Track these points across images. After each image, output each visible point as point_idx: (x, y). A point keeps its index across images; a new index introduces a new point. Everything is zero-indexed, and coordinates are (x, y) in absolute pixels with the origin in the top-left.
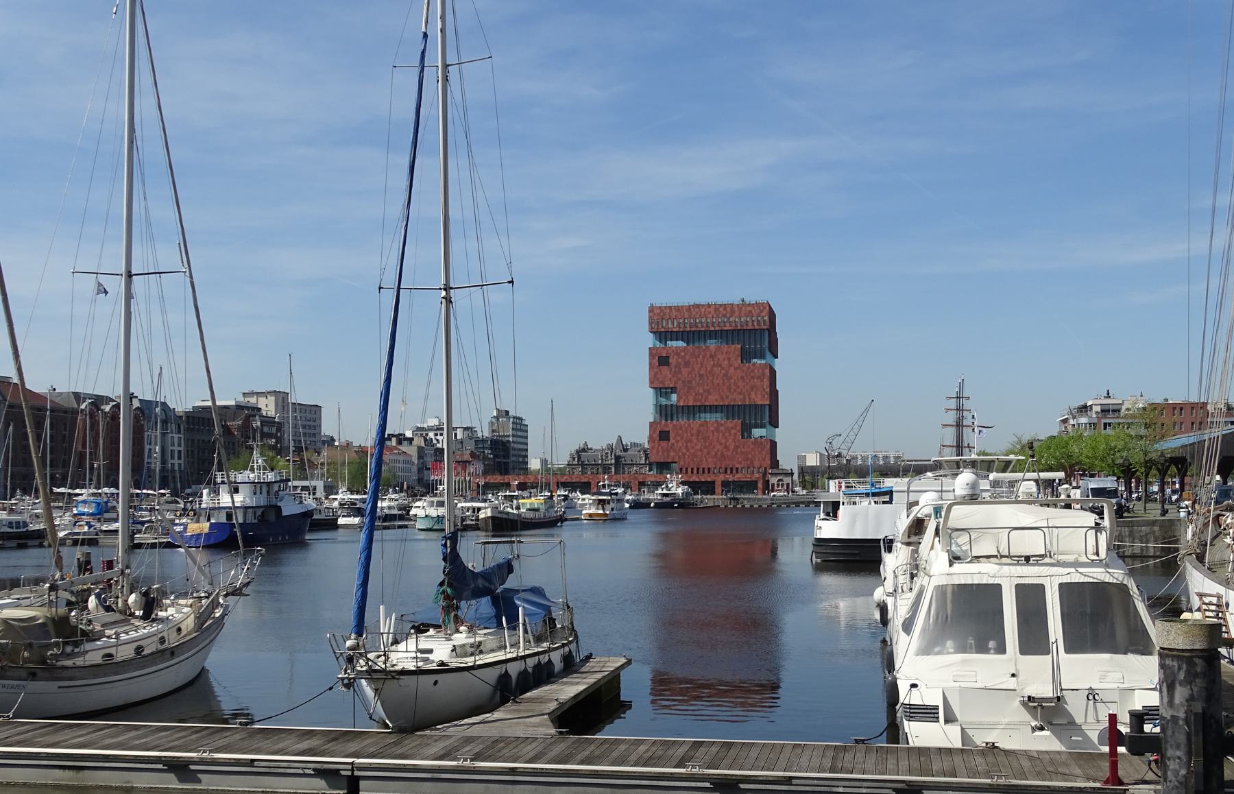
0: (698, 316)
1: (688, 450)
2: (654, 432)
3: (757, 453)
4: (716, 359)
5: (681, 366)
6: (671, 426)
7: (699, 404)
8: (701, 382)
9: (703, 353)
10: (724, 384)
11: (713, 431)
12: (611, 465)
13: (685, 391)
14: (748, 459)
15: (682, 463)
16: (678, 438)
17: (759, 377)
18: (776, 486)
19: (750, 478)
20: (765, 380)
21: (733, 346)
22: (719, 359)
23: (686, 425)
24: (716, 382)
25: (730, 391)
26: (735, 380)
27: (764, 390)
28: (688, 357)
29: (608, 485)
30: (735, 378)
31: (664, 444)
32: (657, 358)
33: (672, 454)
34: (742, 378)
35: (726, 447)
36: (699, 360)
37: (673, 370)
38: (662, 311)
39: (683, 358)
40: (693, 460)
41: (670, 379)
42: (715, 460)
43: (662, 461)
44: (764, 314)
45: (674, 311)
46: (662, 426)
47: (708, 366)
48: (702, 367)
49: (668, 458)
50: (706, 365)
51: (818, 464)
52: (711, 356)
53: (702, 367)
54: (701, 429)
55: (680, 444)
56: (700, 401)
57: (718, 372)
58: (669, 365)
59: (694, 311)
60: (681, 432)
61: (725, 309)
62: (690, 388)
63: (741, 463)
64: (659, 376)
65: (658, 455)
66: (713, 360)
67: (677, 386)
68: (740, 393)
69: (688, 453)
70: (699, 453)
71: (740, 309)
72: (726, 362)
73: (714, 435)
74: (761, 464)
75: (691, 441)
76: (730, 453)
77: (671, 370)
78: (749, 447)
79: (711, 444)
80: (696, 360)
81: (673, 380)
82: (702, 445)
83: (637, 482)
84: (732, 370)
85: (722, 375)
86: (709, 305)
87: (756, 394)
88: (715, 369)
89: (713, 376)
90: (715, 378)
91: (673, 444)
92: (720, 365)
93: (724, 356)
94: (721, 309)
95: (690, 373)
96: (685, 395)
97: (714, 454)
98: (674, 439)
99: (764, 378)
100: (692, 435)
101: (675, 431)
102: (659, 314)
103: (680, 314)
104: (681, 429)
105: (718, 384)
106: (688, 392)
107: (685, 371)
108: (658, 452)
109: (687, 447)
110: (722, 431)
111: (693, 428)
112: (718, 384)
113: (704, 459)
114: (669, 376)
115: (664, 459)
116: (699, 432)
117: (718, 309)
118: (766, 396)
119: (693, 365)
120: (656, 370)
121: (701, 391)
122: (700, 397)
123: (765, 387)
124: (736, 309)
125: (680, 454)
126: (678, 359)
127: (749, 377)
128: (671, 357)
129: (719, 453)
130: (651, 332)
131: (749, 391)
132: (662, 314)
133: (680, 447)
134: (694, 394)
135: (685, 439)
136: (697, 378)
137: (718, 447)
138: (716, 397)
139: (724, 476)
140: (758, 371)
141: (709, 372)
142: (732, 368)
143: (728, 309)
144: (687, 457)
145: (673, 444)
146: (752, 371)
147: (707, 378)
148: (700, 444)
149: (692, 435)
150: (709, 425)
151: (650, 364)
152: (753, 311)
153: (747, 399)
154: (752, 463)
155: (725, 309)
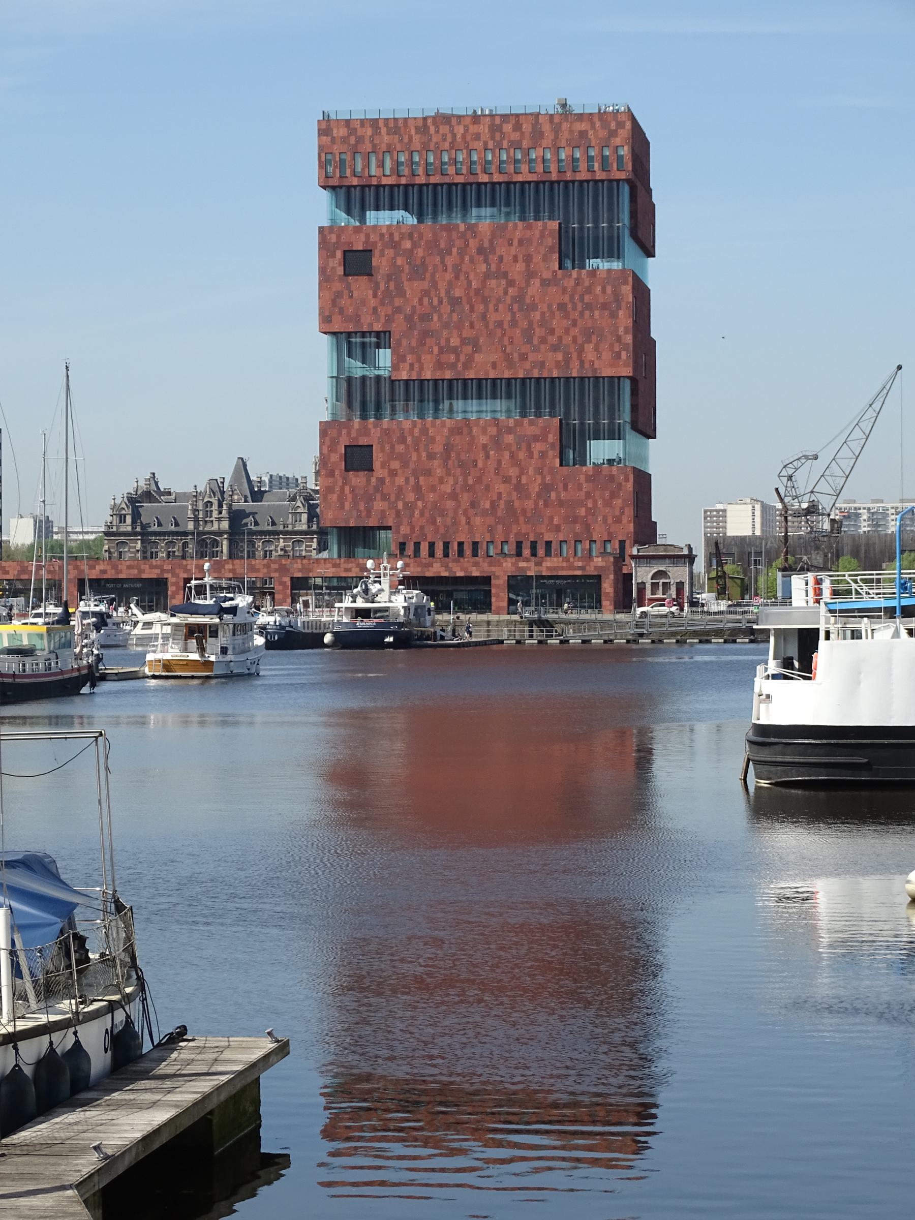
0: (446, 145)
2: (332, 449)
3: (600, 502)
4: (494, 259)
5: (404, 277)
6: (375, 433)
7: (448, 375)
8: (455, 317)
10: (514, 323)
11: (485, 447)
12: (220, 533)
13: (414, 343)
14: (575, 520)
15: (404, 529)
16: (395, 465)
17: (604, 306)
18: (648, 587)
19: (582, 568)
20: (621, 313)
21: (540, 223)
22: (501, 258)
23: (416, 431)
24: (493, 317)
25: (529, 341)
26: (543, 314)
27: (619, 339)
29: (211, 586)
30: (543, 307)
31: (358, 479)
32: (339, 254)
33: (379, 505)
34: (562, 307)
35: (519, 488)
36: (450, 261)
37: (382, 286)
38: (353, 131)
40: (434, 522)
41: (375, 310)
42: (490, 520)
43: (352, 524)
44: (617, 141)
45: (384, 130)
46: (354, 434)
47: (472, 277)
48: (457, 277)
49: (369, 515)
50: (466, 273)
51: (758, 533)
52: (481, 250)
53: (457, 277)
55: (400, 480)
56: (453, 366)
58: (370, 275)
59: (437, 132)
60: (400, 448)
61: (517, 127)
62: (425, 334)
63: (558, 529)
64: (344, 301)
65: (342, 507)
66: (486, 261)
67: (394, 327)
68: (555, 348)
69: (420, 503)
70: (450, 504)
71: (557, 130)
72: (520, 266)
73: (487, 457)
74: (610, 534)
75: (428, 473)
76: (529, 504)
77: (377, 285)
79: (479, 480)
80: (443, 261)
82: (456, 483)
83: (287, 580)
84: (535, 287)
85: (508, 301)
86: (476, 118)
87: (596, 349)
88: (493, 283)
89: (485, 301)
91: (381, 481)
92: (505, 275)
93: (513, 250)
96: (412, 353)
97: (487, 505)
98: (383, 465)
99: (619, 308)
100: (431, 456)
101: (387, 447)
102: (344, 140)
103: (401, 141)
104: (402, 440)
105: (500, 324)
106: (421, 343)
107: (413, 289)
109: (417, 488)
111: (433, 440)
112: (500, 324)
113: (463, 520)
114: (373, 302)
115: (359, 517)
116: (448, 448)
117: (500, 128)
118: (624, 355)
119: (433, 275)
120: (337, 286)
121: (455, 341)
122: (452, 357)
123: (621, 331)
124: (546, 128)
125: (400, 505)
126: (394, 258)
127: (579, 308)
128: (376, 253)
129: (502, 504)
130: (324, 187)
131: (580, 341)
132: (352, 140)
133: (400, 489)
134: (436, 350)
135: (412, 466)
136: (446, 308)
137: (499, 487)
138: (495, 357)
139: (514, 564)
140: (604, 291)
141: (477, 292)
142: (536, 282)
143: (527, 127)
144: (417, 512)
145: (381, 481)
146: (589, 290)
147: (472, 310)
148: (451, 480)
149: (431, 456)
150: (475, 430)
151: (322, 270)
152: (590, 133)
153: (575, 364)
154: (587, 527)
155: (517, 127)
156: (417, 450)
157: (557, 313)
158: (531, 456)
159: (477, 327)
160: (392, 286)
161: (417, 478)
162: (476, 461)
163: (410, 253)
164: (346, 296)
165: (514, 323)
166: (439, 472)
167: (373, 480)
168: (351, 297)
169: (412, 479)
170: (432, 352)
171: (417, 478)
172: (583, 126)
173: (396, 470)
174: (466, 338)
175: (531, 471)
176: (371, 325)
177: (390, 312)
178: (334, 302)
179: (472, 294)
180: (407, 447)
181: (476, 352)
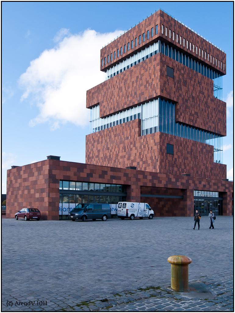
1: (185, 168)
3: (221, 175)
9: (194, 77)
11: (199, 151)
17: (222, 113)
22: (203, 87)
23: (185, 142)
25: (208, 118)
26: (211, 110)
28: (185, 76)
30: (211, 108)
36: (192, 82)
39: (183, 75)
41: (175, 92)
47: (197, 91)
52: (199, 83)
54: (193, 148)
56: (193, 121)
60: (181, 148)
61: (206, 45)
64: (167, 86)
65: (166, 168)
68: (213, 122)
71: (213, 51)
73: (200, 156)
75: (187, 159)
77: (175, 84)
78: (218, 170)
80: (190, 82)
81: (177, 94)
88: (201, 95)
90: (201, 103)
91: (176, 159)
92: (203, 94)
94: (204, 43)
95: (187, 92)
107: (184, 88)
108: (165, 165)
110: (204, 152)
111: (188, 147)
112: (203, 109)
120: (165, 79)
124: (212, 49)
128: (175, 70)
133: (180, 163)
134: (189, 113)
136: (191, 99)
141: (198, 96)
142: (209, 98)
146: (219, 106)
149: (188, 152)
151: (161, 70)
152: (219, 56)
156: (184, 150)
157: (214, 111)
158: (209, 158)
160: (179, 86)
161: (184, 160)
162: (198, 157)
163: (183, 75)
164: (167, 84)
165: (205, 112)
166: (190, 159)
167: (174, 159)
168: (168, 85)
169: (183, 160)
170: (188, 114)
171: (184, 160)
172: (218, 53)
173: (179, 156)
174: (196, 112)
175: (209, 162)
176: (173, 98)
177: (178, 95)
178: (164, 86)
179: (197, 97)
180: (182, 148)
181: (197, 118)
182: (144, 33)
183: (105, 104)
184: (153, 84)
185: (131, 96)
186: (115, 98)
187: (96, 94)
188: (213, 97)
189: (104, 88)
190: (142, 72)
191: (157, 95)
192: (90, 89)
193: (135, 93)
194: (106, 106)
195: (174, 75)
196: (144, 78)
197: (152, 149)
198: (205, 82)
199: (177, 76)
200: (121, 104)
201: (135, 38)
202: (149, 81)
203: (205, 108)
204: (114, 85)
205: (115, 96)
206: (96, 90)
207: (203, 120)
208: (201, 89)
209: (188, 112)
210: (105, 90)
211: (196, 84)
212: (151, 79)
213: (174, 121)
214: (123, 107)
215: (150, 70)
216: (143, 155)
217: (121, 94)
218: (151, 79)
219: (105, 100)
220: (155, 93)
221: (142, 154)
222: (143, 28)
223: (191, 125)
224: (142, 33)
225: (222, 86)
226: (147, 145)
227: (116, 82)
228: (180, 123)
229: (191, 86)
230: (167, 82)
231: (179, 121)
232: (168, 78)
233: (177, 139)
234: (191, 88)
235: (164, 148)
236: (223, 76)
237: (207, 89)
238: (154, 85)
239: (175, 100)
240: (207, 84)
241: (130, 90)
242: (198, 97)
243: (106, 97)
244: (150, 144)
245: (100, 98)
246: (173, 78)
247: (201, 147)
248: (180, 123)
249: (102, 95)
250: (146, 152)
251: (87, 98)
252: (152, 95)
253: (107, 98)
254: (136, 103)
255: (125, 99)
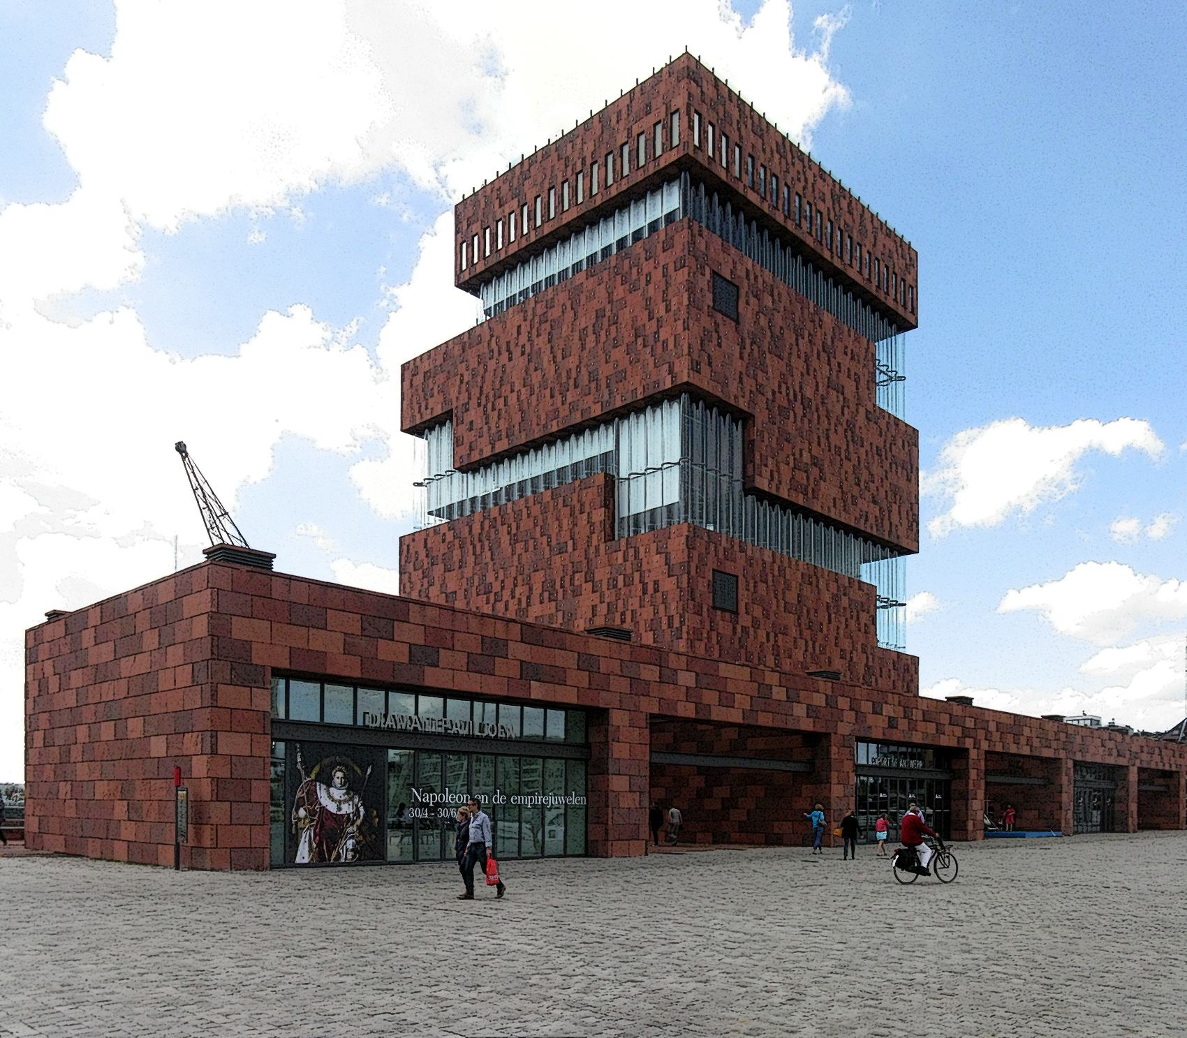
22: (839, 364)
28: (778, 320)
57: (839, 407)
77: (743, 347)
81: (749, 384)
88: (833, 393)
94: (844, 204)
95: (783, 380)
124: (869, 226)
142: (862, 410)
159: (823, 446)
168: (720, 345)
170: (788, 464)
172: (890, 244)
177: (754, 389)
179: (819, 401)
182: (627, 143)
183: (474, 414)
184: (661, 339)
185: (576, 387)
186: (515, 394)
187: (441, 378)
188: (875, 405)
189: (472, 355)
190: (620, 292)
191: (679, 382)
192: (415, 360)
193: (593, 377)
194: (479, 423)
195: (740, 310)
196: (625, 316)
197: (656, 590)
198: (846, 347)
199: (749, 315)
200: (538, 417)
201: (589, 161)
202: (644, 325)
203: (848, 445)
204: (508, 343)
205: (512, 384)
206: (438, 363)
207: (841, 487)
208: (834, 373)
209: (788, 457)
210: (473, 363)
211: (815, 352)
212: (654, 321)
213: (738, 486)
214: (545, 426)
215: (651, 286)
216: (623, 614)
217: (536, 378)
218: (654, 321)
219: (474, 402)
220: (671, 372)
221: (620, 609)
222: (622, 123)
223: (801, 503)
224: (619, 143)
225: (904, 368)
226: (637, 575)
227: (519, 333)
228: (761, 495)
229: (799, 357)
230: (715, 335)
231: (758, 486)
232: (720, 322)
233: (749, 553)
234: (799, 365)
235: (702, 586)
236: (908, 333)
237: (855, 374)
238: (665, 342)
239: (743, 404)
240: (852, 358)
241: (572, 362)
242: (823, 403)
243: (478, 390)
244: (650, 571)
245: (453, 393)
246: (738, 323)
247: (833, 586)
248: (761, 495)
249: (461, 382)
250: (634, 603)
251: (402, 394)
252: (657, 383)
253: (481, 393)
254: (597, 411)
255: (552, 397)
